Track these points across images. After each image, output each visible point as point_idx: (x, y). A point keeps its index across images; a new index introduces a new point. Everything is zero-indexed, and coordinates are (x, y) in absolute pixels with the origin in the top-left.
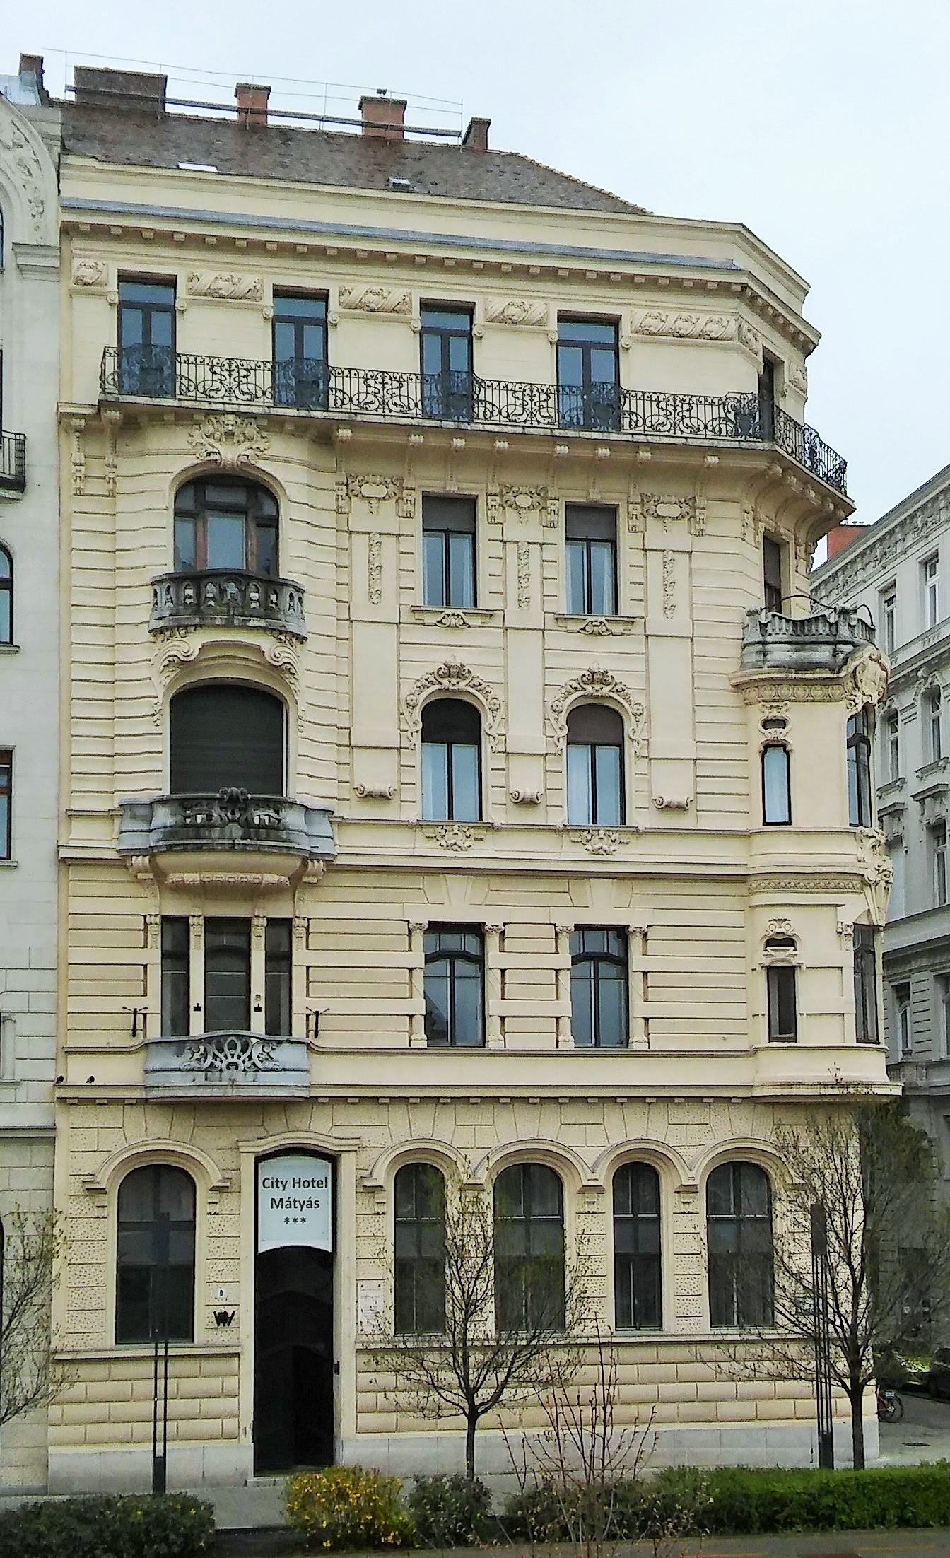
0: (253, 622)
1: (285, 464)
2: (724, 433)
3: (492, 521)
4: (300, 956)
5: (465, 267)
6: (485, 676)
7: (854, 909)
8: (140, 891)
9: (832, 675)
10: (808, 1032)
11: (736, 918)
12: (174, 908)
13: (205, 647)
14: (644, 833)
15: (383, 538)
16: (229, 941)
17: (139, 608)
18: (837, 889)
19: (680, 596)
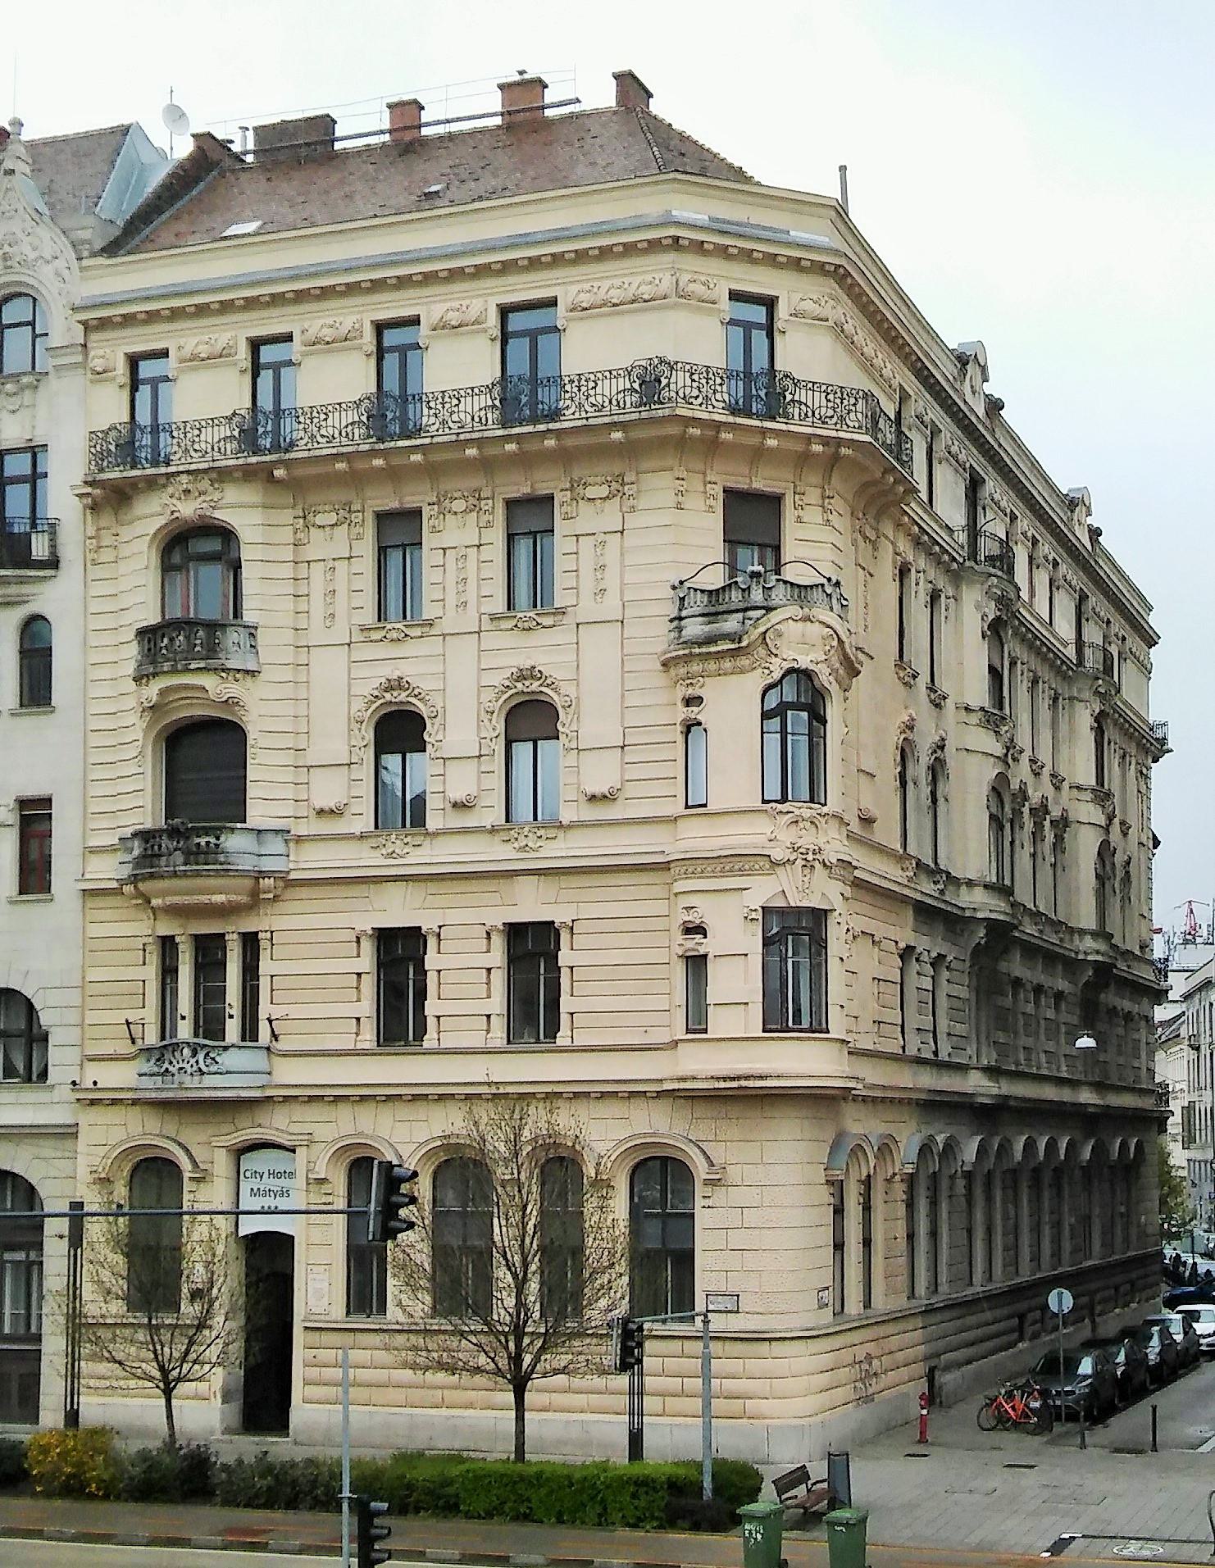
1: (241, 511)
2: (628, 405)
4: (266, 966)
5: (403, 282)
6: (425, 685)
7: (763, 891)
8: (133, 914)
9: (733, 646)
10: (720, 1023)
11: (661, 907)
12: (164, 929)
13: (163, 693)
14: (570, 827)
15: (336, 563)
16: (209, 952)
18: (742, 873)
19: (611, 580)
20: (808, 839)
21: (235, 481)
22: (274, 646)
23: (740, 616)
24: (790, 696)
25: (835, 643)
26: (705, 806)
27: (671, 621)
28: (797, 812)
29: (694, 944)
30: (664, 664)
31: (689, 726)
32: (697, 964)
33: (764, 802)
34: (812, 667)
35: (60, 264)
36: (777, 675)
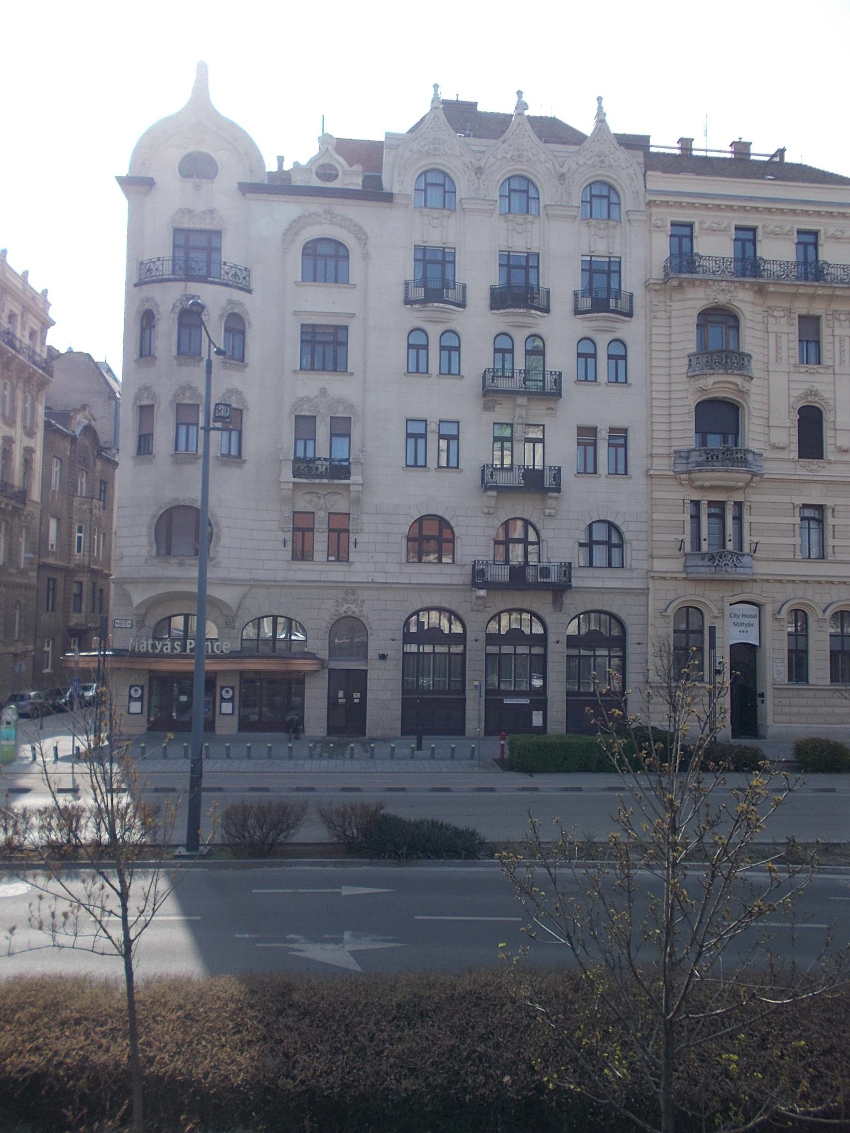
0: (735, 372)
3: (828, 326)
4: (747, 518)
6: (826, 395)
12: (696, 497)
16: (718, 510)
17: (681, 366)
21: (744, 288)
22: (756, 367)
35: (630, 171)
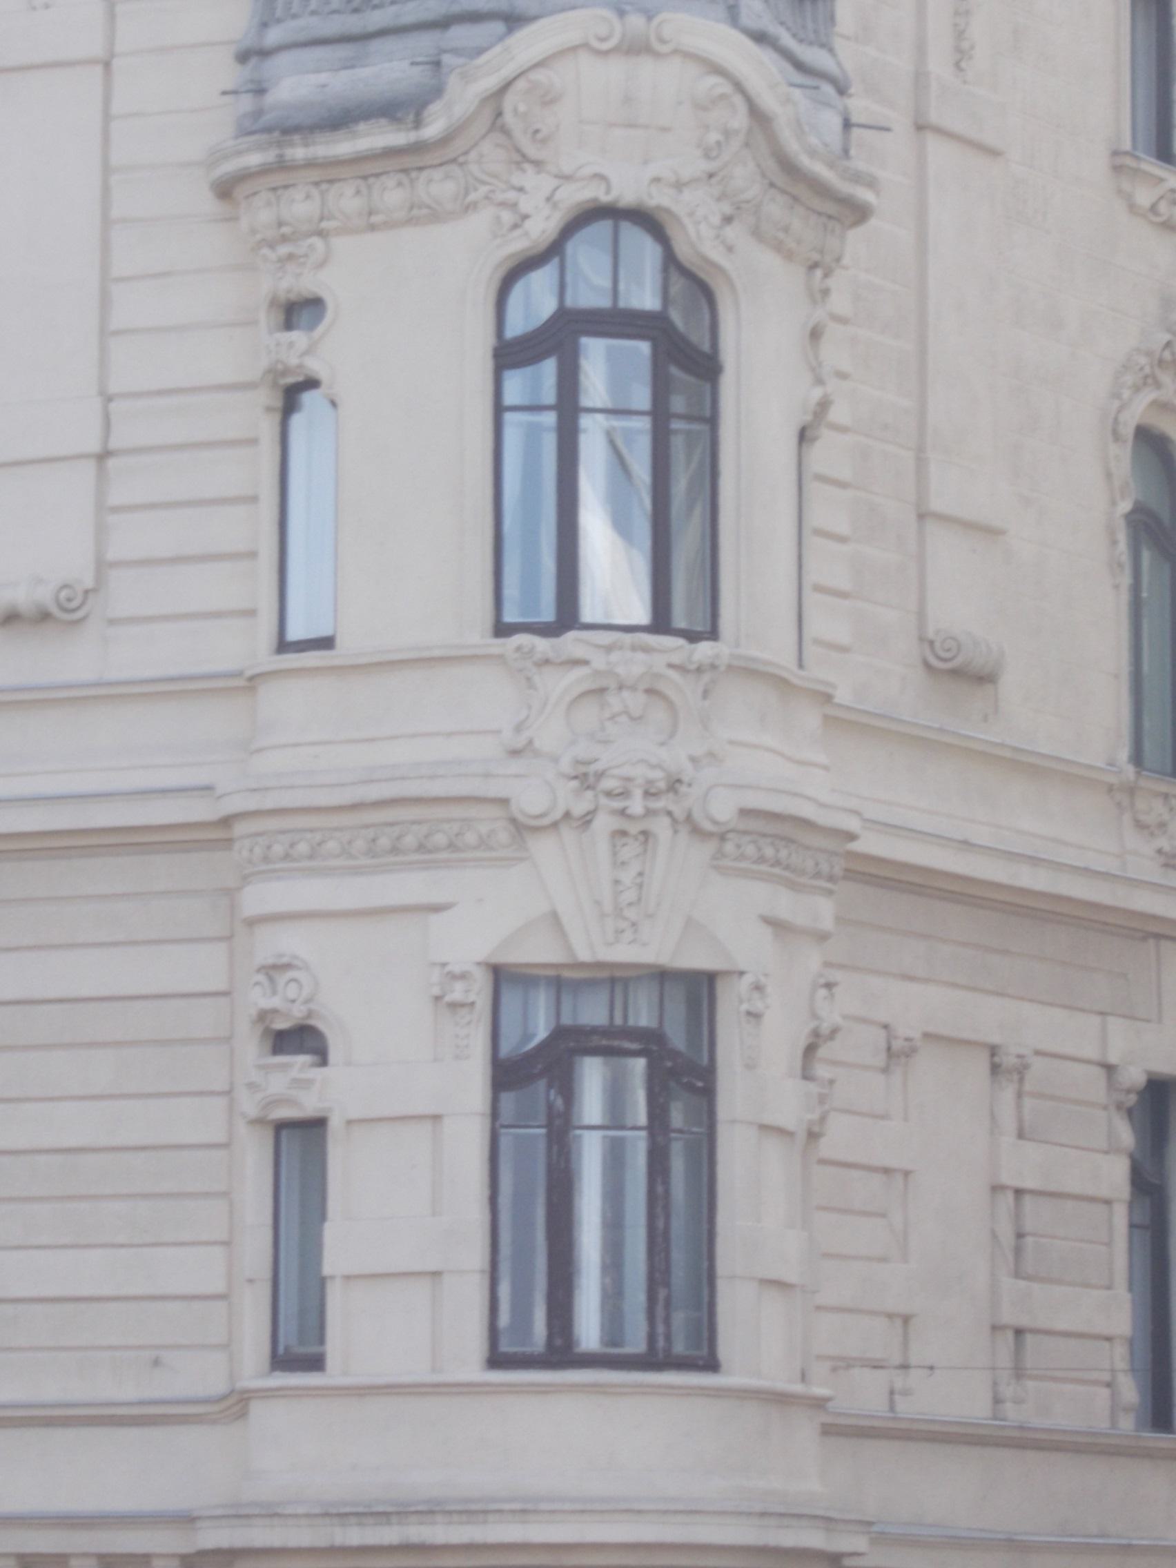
7: (493, 914)
11: (203, 967)
18: (426, 854)
20: (634, 752)
23: (425, 42)
24: (590, 291)
25: (740, 120)
26: (326, 643)
27: (243, 57)
28: (599, 661)
29: (297, 1086)
30: (225, 190)
31: (293, 393)
32: (301, 1141)
33: (502, 630)
34: (658, 198)
36: (542, 227)
